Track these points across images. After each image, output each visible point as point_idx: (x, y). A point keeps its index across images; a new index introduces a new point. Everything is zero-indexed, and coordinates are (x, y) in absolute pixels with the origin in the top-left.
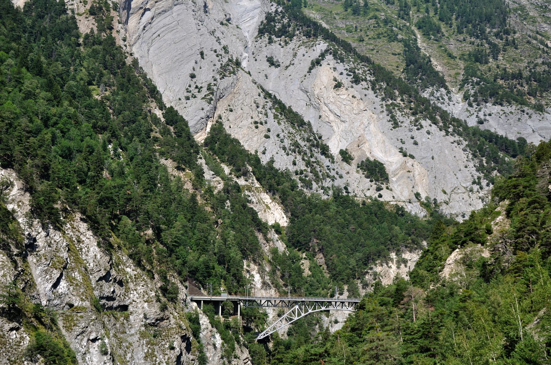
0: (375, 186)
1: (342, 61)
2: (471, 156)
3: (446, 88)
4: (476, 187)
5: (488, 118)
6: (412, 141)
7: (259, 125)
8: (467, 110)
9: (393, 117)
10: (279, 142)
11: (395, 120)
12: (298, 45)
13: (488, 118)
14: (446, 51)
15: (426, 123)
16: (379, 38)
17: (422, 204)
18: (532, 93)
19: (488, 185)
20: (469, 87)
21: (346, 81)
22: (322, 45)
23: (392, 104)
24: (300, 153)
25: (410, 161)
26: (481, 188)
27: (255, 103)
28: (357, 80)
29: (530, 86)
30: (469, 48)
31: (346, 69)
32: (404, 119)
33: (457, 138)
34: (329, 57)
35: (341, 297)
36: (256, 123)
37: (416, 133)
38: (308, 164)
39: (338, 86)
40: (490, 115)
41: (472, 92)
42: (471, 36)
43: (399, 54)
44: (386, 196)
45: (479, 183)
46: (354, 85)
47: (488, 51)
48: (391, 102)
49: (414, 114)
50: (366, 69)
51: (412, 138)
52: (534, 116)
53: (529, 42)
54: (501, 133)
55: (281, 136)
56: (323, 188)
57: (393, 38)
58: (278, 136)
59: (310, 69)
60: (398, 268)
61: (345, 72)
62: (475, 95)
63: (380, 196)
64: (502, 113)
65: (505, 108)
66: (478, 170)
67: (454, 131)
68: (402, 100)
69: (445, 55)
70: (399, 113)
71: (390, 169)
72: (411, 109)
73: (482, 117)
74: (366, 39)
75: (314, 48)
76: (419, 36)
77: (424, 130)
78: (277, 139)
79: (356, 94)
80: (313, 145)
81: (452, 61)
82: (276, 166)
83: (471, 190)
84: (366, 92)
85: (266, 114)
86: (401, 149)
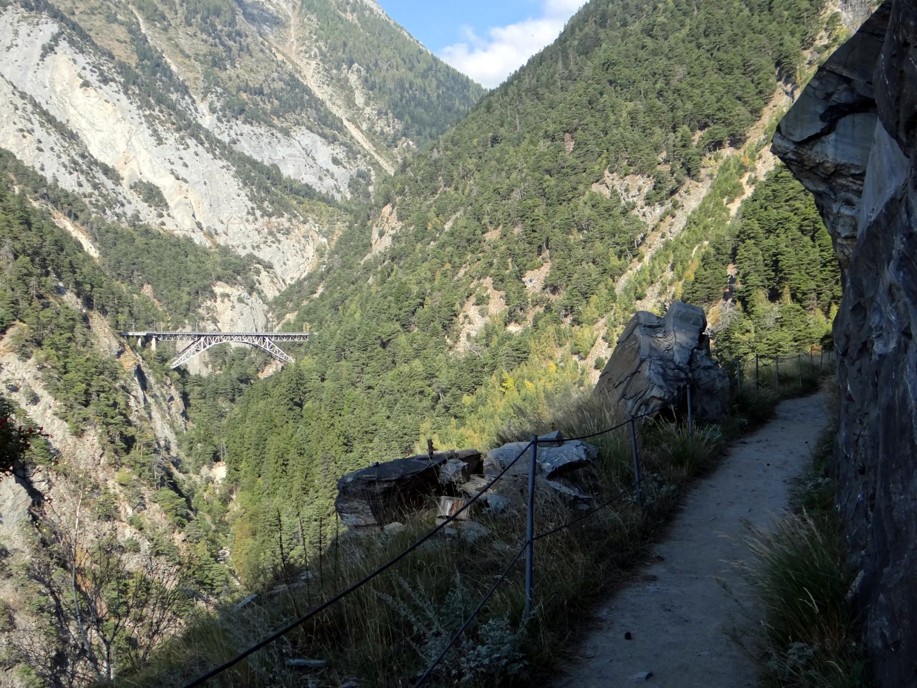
0: (155, 212)
1: (83, 52)
2: (241, 185)
3: (191, 97)
4: (251, 218)
5: (239, 137)
6: (181, 162)
7: (26, 134)
8: (218, 127)
9: (155, 131)
10: (55, 158)
11: (158, 135)
12: (16, 20)
13: (239, 137)
14: (177, 46)
15: (192, 142)
16: (93, 13)
17: (205, 234)
18: (275, 113)
19: (262, 216)
20: (211, 97)
21: (93, 78)
22: (50, 28)
23: (150, 115)
24: (82, 172)
25: (185, 186)
26: (256, 219)
27: (12, 103)
28: (105, 80)
29: (272, 103)
30: (204, 49)
31: (88, 63)
32: (168, 135)
33: (225, 163)
34: (63, 44)
35: (184, 331)
36: (21, 130)
37: (183, 153)
38: (95, 186)
39: (86, 84)
40: (241, 135)
41: (218, 105)
42: (202, 32)
43: (125, 42)
44: (170, 226)
45: (254, 214)
46: (102, 85)
47: (224, 55)
48: (147, 112)
49: (179, 130)
50: (111, 65)
51: (181, 158)
52: (282, 140)
53: (262, 51)
54: (256, 157)
55: (56, 148)
56: (117, 215)
57: (111, 19)
58: (52, 149)
59: (43, 56)
60: (223, 302)
61: (88, 67)
62: (223, 109)
63: (163, 224)
64: (252, 133)
65: (254, 129)
66: (251, 200)
67: (221, 154)
68: (161, 111)
69: (177, 51)
70: (160, 128)
71: (166, 195)
72: (173, 124)
73: (235, 137)
74: (77, 12)
75: (40, 27)
76: (141, 20)
77: (192, 150)
78: (52, 153)
79: (106, 97)
80: (92, 163)
81: (187, 61)
82: (61, 185)
83: (247, 221)
84: (117, 96)
85: (30, 120)
86: (172, 170)
